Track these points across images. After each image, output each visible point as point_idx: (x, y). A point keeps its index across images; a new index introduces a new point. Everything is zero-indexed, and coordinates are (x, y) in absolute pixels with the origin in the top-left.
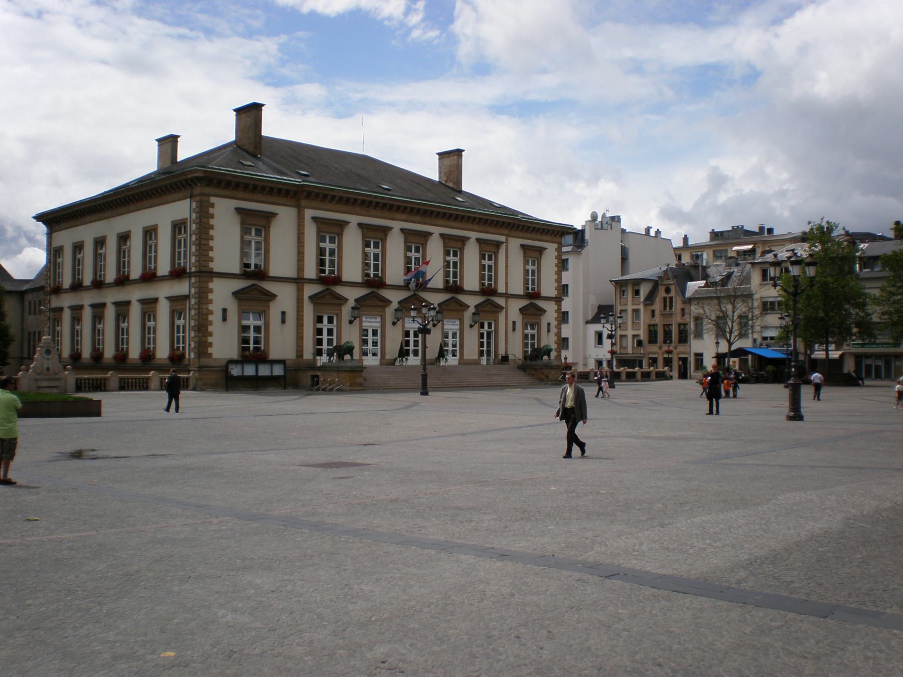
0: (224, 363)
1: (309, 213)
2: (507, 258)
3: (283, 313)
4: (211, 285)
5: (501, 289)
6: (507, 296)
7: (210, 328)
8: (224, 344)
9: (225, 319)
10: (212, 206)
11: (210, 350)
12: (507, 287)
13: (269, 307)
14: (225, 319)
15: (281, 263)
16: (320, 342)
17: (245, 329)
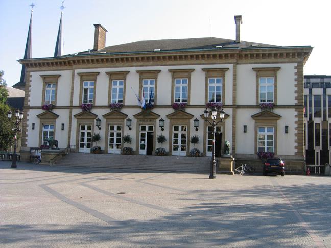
0: (29, 150)
1: (77, 71)
2: (235, 79)
3: (63, 125)
4: (28, 113)
5: (228, 100)
6: (235, 107)
7: (27, 133)
8: (33, 139)
9: (33, 128)
10: (31, 76)
11: (26, 143)
12: (234, 99)
13: (55, 122)
14: (33, 128)
15: (62, 100)
16: (83, 140)
17: (46, 133)
